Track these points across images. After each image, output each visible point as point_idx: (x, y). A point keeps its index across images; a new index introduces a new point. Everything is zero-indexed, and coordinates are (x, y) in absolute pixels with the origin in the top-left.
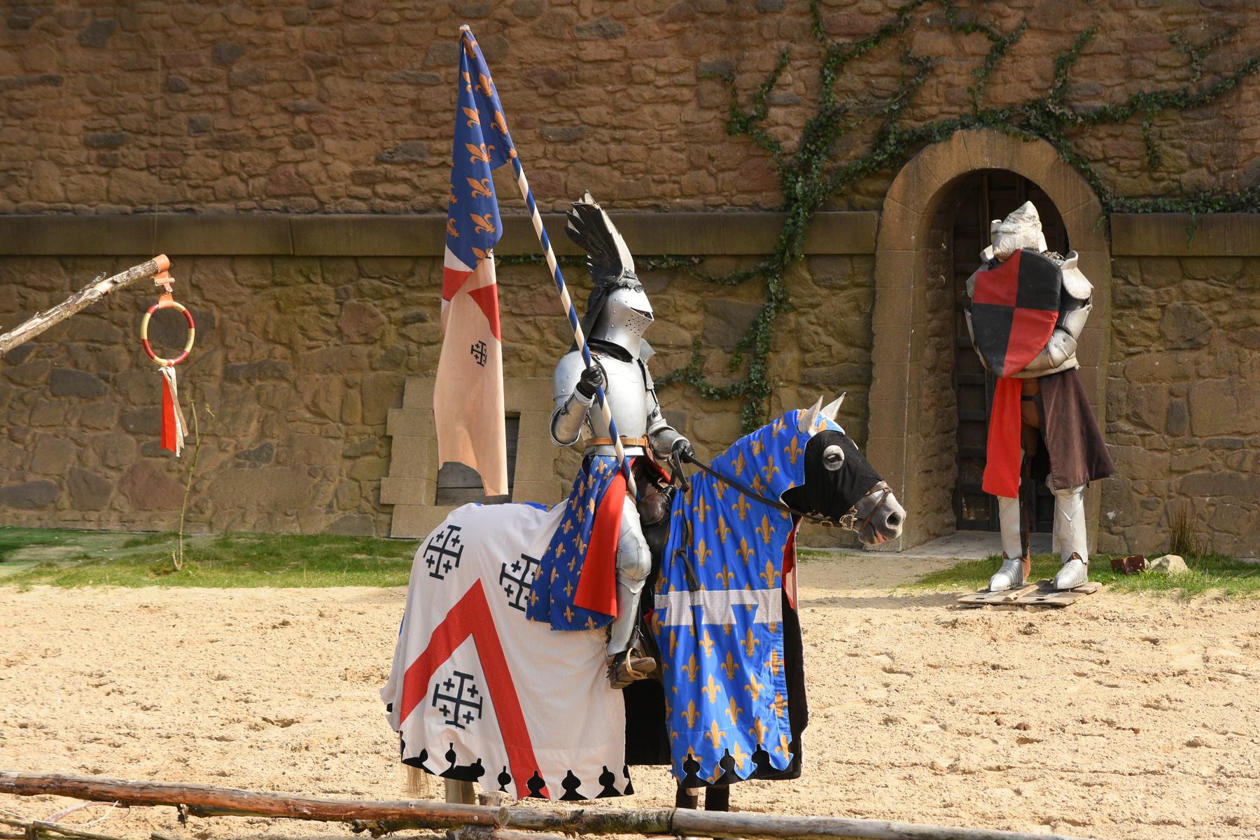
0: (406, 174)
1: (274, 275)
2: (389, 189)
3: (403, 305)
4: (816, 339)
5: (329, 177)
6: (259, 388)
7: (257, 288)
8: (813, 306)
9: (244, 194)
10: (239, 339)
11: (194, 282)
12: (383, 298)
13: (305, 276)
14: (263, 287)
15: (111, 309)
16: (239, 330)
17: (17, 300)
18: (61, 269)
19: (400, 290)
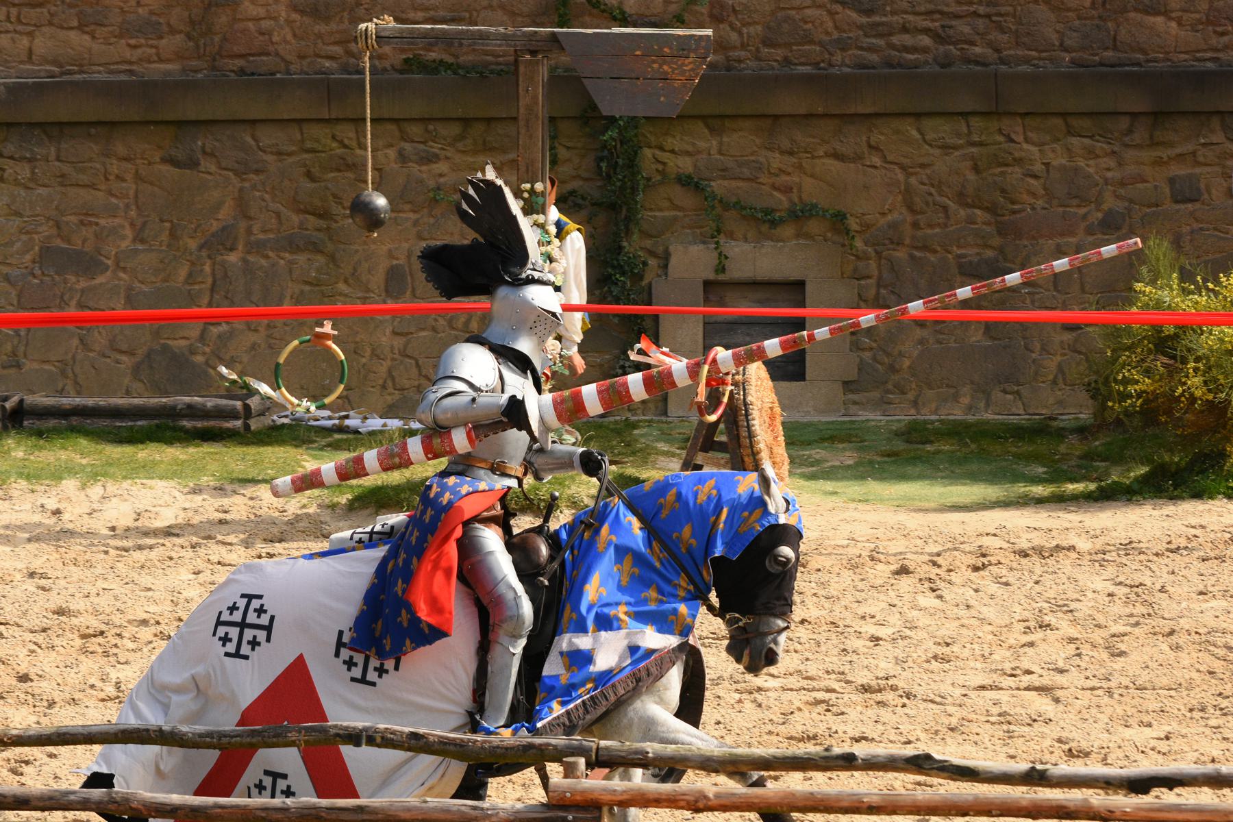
0: (928, 24)
1: (970, 133)
2: (907, 39)
3: (1120, 165)
4: (930, 199)
5: (836, 28)
6: (291, 262)
7: (947, 148)
8: (923, 166)
9: (738, 44)
10: (264, 210)
11: (873, 143)
12: (1097, 157)
13: (1004, 135)
14: (956, 148)
15: (107, 179)
16: (264, 200)
17: (654, 166)
18: (44, 137)
19: (1116, 149)
